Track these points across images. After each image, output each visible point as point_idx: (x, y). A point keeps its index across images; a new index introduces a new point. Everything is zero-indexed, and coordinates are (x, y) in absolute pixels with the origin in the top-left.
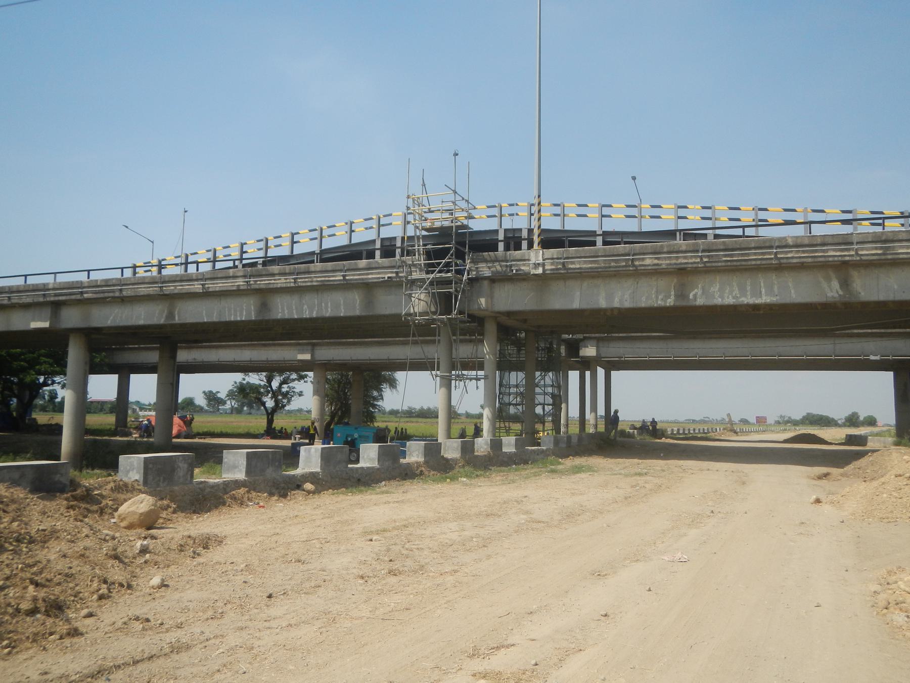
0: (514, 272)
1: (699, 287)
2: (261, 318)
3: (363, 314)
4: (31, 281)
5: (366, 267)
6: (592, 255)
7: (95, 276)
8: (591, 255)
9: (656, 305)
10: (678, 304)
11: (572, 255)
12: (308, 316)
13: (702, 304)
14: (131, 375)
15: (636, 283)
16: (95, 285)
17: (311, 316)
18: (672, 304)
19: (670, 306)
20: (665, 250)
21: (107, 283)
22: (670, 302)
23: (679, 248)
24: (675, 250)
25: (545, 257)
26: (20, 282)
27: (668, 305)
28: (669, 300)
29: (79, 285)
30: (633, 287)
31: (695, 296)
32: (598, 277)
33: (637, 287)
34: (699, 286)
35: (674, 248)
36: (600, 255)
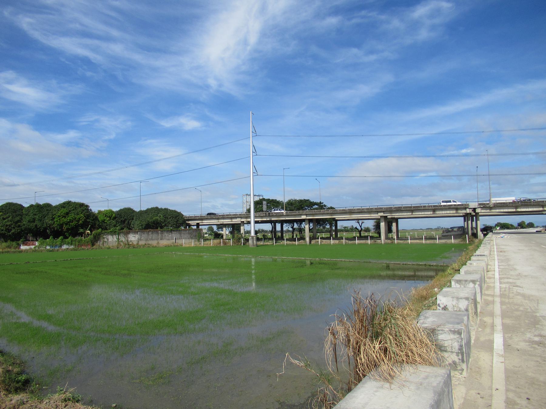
4: (379, 207)
7: (395, 206)
16: (396, 208)
21: (399, 207)
26: (376, 207)
29: (392, 208)
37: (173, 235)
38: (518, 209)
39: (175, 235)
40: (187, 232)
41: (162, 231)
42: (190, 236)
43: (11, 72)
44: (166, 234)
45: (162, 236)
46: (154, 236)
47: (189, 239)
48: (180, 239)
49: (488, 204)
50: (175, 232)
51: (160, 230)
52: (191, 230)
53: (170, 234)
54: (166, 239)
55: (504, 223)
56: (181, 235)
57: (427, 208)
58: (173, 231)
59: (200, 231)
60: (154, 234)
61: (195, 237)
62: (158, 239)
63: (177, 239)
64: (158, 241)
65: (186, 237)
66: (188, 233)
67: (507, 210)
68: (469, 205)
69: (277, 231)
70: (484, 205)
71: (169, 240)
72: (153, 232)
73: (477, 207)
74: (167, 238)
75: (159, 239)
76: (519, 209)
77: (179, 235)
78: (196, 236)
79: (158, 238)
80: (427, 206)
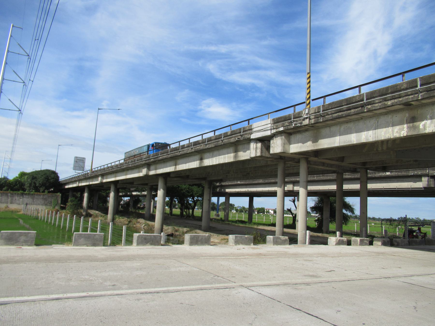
0: (293, 125)
1: (427, 117)
2: (200, 166)
3: (234, 161)
5: (231, 134)
6: (339, 105)
8: (338, 106)
9: (392, 137)
10: (410, 134)
11: (326, 108)
12: (215, 164)
13: (431, 131)
14: (230, 197)
15: (377, 122)
17: (216, 164)
18: (405, 135)
19: (404, 136)
20: (390, 91)
22: (403, 134)
23: (401, 87)
24: (397, 90)
25: (311, 113)
27: (402, 136)
28: (403, 132)
30: (375, 125)
31: (424, 126)
32: (351, 122)
33: (378, 126)
34: (428, 116)
35: (397, 88)
36: (343, 104)
37: (25, 199)
38: (421, 125)
39: (26, 199)
40: (42, 197)
41: (12, 194)
42: (44, 202)
43: (212, 99)
44: (17, 198)
45: (12, 199)
46: (3, 198)
47: (42, 205)
48: (32, 204)
49: (298, 116)
50: (27, 196)
51: (10, 193)
52: (46, 194)
53: (21, 197)
54: (17, 204)
55: (33, 173)
56: (34, 200)
57: (186, 151)
58: (26, 194)
59: (57, 197)
60: (3, 197)
61: (49, 203)
62: (7, 203)
63: (29, 204)
64: (7, 204)
65: (39, 203)
66: (43, 198)
67: (371, 133)
68: (251, 129)
69: (374, 219)
70: (286, 123)
71: (19, 204)
72: (3, 194)
73: (268, 133)
74: (18, 202)
75: (9, 203)
76: (428, 122)
77: (31, 200)
78: (51, 202)
79: (8, 202)
80: (186, 146)
